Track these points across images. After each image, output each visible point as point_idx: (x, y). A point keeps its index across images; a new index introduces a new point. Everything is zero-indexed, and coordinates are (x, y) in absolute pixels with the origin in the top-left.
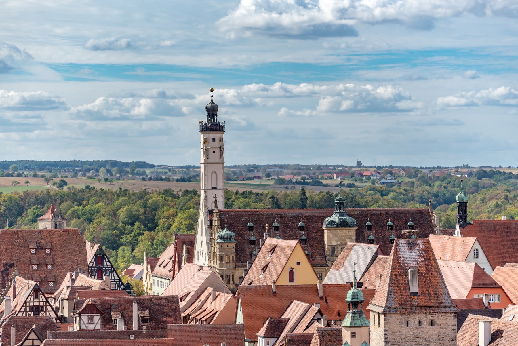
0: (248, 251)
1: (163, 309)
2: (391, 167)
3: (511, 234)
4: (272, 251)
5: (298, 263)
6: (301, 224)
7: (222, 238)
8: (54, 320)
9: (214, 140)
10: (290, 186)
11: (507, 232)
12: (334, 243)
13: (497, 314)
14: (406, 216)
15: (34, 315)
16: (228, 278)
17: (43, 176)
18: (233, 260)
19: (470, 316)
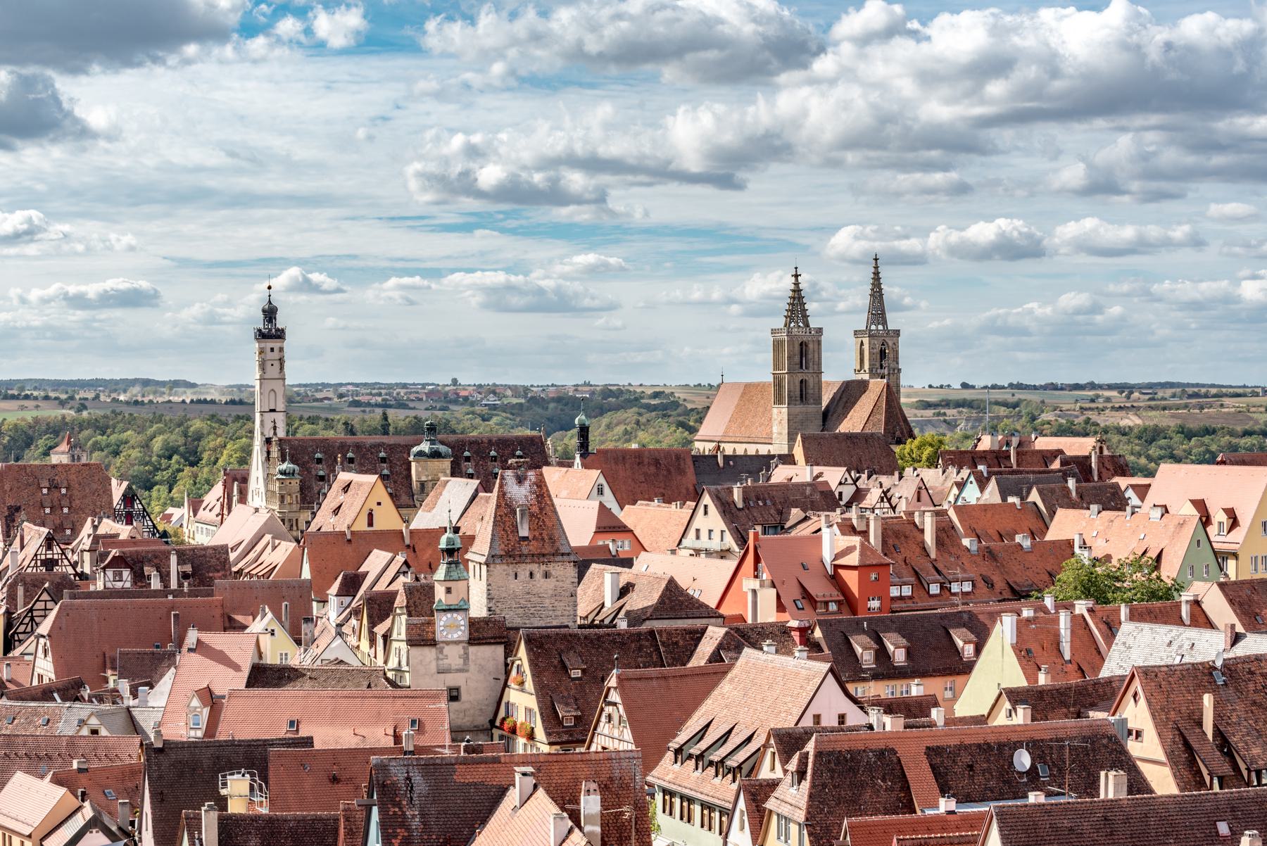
0: (316, 489)
2: (494, 385)
4: (346, 489)
5: (379, 504)
6: (382, 454)
7: (283, 473)
9: (272, 350)
10: (368, 409)
12: (424, 479)
13: (628, 563)
16: (291, 524)
17: (56, 398)
19: (594, 565)
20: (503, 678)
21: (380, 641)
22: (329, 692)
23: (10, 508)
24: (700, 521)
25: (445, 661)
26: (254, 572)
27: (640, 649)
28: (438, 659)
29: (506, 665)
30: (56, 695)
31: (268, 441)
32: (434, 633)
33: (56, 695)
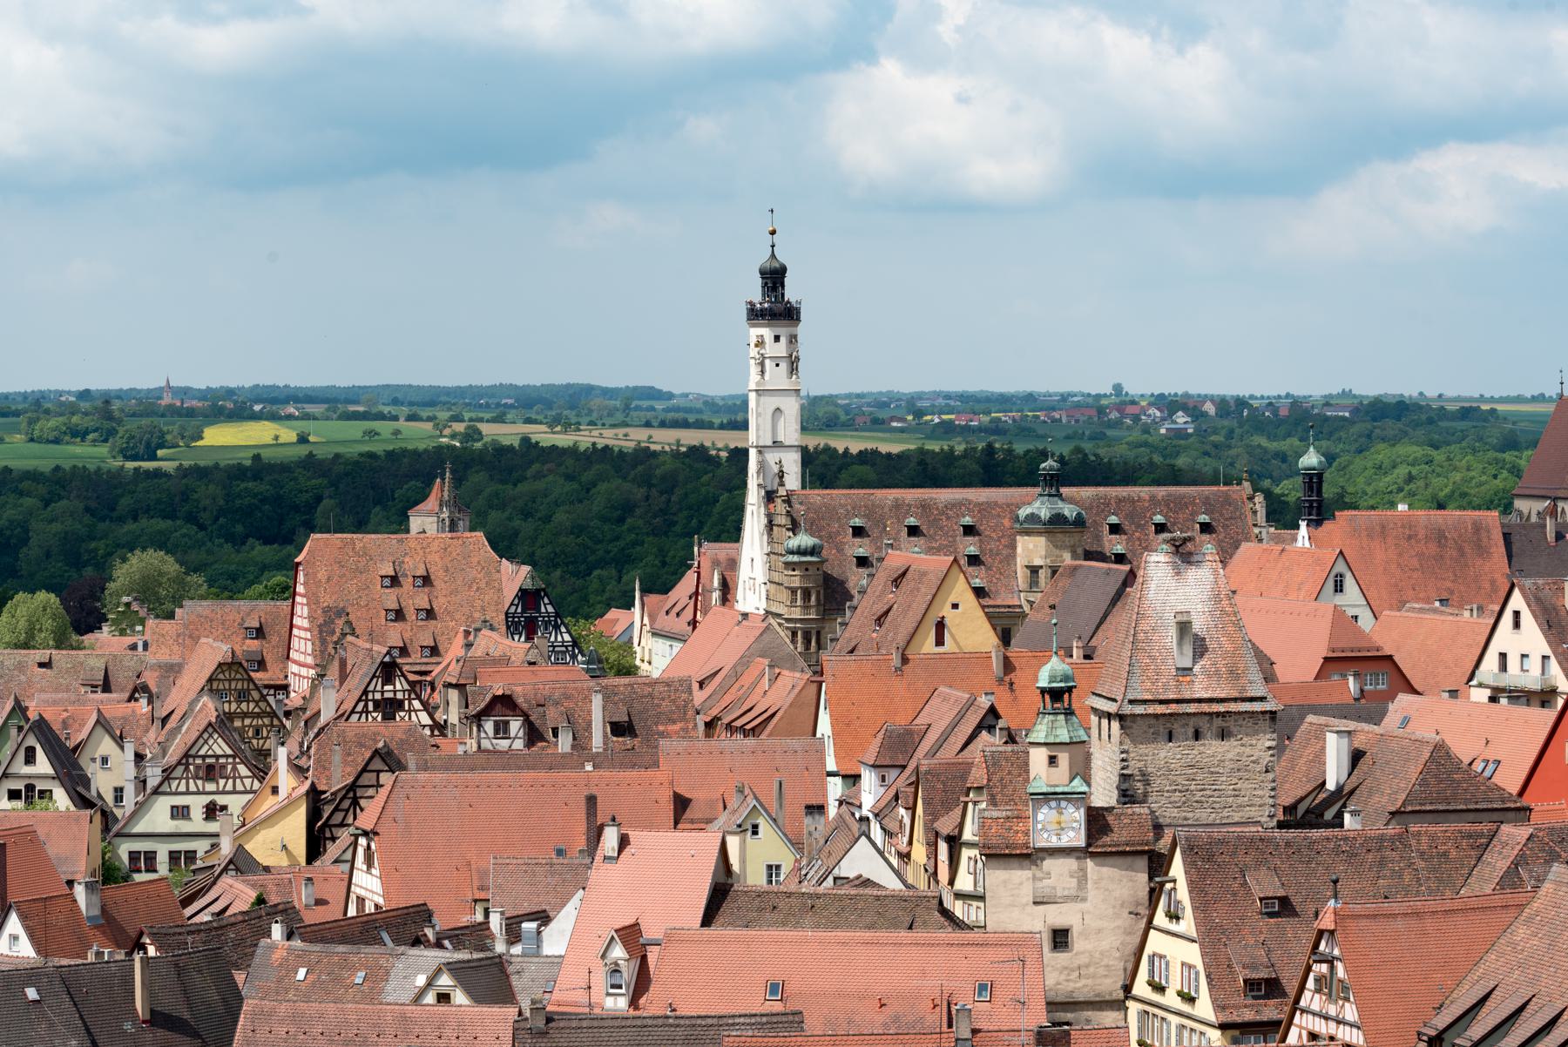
1: (659, 706)
3: (1418, 541)
4: (898, 580)
5: (955, 606)
6: (967, 520)
8: (427, 732)
11: (1410, 537)
12: (1037, 562)
14: (1193, 503)
15: (384, 718)
18: (818, 599)
19: (1310, 718)
20: (1144, 911)
21: (943, 847)
22: (841, 934)
23: (327, 610)
24: (1504, 637)
25: (1046, 882)
26: (738, 723)
27: (1382, 863)
28: (1034, 878)
29: (1152, 891)
30: (385, 936)
31: (770, 497)
32: (1027, 834)
33: (385, 936)
